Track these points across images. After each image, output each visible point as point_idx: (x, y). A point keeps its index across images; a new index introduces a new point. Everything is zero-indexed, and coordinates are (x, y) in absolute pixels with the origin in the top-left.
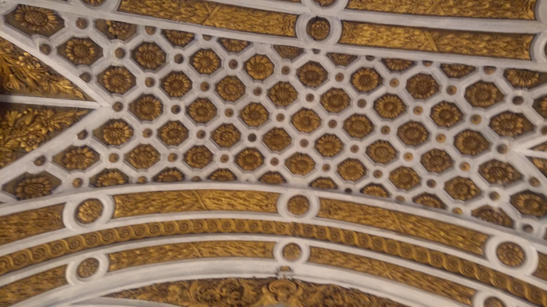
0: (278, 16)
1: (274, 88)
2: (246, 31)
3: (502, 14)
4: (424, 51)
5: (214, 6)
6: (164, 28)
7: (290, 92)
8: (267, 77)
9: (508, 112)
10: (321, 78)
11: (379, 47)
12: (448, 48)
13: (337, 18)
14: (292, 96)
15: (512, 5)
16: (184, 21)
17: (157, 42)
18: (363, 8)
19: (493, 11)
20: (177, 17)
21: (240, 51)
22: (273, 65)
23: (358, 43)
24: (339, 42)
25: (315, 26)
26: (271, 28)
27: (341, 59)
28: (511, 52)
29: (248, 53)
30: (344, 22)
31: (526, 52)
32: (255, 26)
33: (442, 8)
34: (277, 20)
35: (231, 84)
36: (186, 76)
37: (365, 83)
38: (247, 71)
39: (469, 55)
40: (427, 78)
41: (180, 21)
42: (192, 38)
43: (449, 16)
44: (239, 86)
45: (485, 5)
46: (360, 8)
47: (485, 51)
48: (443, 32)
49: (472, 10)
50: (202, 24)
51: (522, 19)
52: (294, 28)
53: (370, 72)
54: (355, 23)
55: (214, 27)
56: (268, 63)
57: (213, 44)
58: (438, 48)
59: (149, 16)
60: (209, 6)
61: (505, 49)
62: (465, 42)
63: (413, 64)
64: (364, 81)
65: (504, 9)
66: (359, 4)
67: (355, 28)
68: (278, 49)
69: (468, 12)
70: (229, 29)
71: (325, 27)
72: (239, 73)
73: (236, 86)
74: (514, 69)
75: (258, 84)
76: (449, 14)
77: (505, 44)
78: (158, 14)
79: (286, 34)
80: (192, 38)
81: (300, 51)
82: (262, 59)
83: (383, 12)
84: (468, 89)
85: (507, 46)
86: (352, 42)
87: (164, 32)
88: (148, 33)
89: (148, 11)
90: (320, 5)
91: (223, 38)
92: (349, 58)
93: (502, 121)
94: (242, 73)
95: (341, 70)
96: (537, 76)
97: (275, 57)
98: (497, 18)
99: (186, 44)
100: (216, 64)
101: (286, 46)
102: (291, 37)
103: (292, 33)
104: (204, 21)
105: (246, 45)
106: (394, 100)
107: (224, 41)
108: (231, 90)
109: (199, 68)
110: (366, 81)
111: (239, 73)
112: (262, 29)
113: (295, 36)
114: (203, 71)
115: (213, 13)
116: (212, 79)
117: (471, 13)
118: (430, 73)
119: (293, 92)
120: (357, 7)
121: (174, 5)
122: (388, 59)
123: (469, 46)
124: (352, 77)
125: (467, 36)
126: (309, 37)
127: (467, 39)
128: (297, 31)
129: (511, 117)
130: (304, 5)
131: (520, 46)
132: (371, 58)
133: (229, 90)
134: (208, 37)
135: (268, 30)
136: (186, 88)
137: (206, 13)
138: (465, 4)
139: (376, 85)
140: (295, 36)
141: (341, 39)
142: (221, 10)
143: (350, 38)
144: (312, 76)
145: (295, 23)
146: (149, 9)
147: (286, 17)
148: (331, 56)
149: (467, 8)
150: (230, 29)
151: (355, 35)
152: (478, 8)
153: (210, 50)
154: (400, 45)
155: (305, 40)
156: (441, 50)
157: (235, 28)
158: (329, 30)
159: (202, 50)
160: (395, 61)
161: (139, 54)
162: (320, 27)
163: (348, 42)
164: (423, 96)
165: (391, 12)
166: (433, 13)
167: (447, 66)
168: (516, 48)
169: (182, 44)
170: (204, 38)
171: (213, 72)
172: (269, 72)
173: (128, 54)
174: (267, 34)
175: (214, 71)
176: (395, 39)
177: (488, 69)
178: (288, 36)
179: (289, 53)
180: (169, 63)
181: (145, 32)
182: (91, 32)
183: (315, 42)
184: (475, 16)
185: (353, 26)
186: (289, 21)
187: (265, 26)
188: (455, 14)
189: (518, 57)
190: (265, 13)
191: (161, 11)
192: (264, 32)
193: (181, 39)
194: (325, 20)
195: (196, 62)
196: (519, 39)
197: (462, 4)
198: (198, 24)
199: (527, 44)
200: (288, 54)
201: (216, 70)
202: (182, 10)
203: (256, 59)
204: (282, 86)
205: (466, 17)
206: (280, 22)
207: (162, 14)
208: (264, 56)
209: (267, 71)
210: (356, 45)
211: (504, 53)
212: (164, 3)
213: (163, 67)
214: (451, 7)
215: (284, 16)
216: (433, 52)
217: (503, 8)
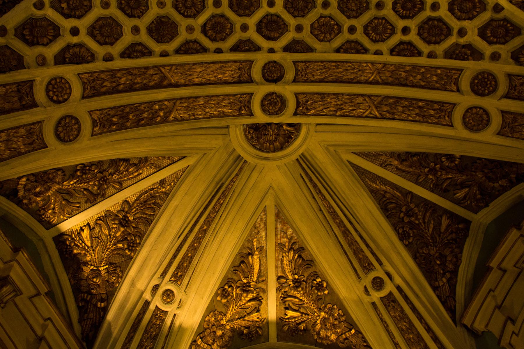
0: (312, 79)
1: (309, 10)
2: (343, 62)
3: (117, 112)
4: (171, 66)
5: (374, 81)
6: (419, 58)
7: (292, 7)
8: (317, 20)
9: (79, 17)
10: (264, 25)
11: (213, 63)
12: (151, 72)
13: (257, 84)
14: (289, 3)
15: (112, 121)
16: (402, 65)
17: (426, 45)
18: (237, 96)
19: (125, 112)
20: (408, 68)
21: (346, 42)
22: (311, 32)
23: (235, 64)
24: (251, 62)
25: (277, 74)
26: (319, 68)
27: (247, 46)
28: (98, 78)
29: (337, 42)
30: (250, 81)
31: (85, 81)
32: (335, 67)
33: (167, 107)
34: (313, 76)
35: (354, 10)
36: (399, 15)
37: (219, 26)
38: (337, 24)
39: (131, 68)
40: (161, 39)
41: (405, 65)
42: (392, 52)
43: (160, 101)
44: (346, 9)
45: (133, 117)
46: (239, 96)
47: (118, 75)
48: (159, 86)
49: (142, 110)
50: (385, 65)
51: (100, 110)
52: (297, 70)
53: (216, 36)
54: (239, 82)
55: (373, 63)
56: (317, 35)
57: (372, 47)
58: (160, 70)
59: (434, 68)
60: (378, 81)
61: (104, 80)
62: (139, 80)
63: (178, 51)
64: (220, 28)
65: (117, 116)
66: (241, 99)
67: (239, 77)
68: (310, 50)
69: (145, 108)
70: (360, 62)
71: (268, 75)
72: (346, 22)
73: (349, 9)
74: (88, 63)
75: (327, 12)
76: (161, 103)
77: (104, 85)
78: (426, 69)
79: (304, 64)
80: (392, 52)
81: (287, 49)
82: (324, 37)
83: (218, 96)
84: (121, 35)
85: (103, 83)
86: (238, 64)
87: (420, 54)
88: (435, 52)
89: (436, 71)
90: (276, 93)
91: (363, 53)
92: (239, 48)
93: (81, 8)
94: (343, 23)
95: (245, 36)
96: (67, 60)
97: (311, 41)
98: (120, 107)
99: (398, 45)
100: (369, 28)
101: (301, 52)
102: (298, 62)
103: (298, 65)
104: (383, 67)
105: (341, 49)
106: (187, 12)
107: (363, 51)
108: (353, 4)
109: (386, 23)
110: (218, 28)
111: (346, 22)
112: (327, 65)
113: (295, 62)
114: (382, 22)
115: (375, 75)
116: (373, 14)
117: (142, 107)
118: (159, 44)
119: (289, 8)
120: (242, 96)
121: (411, 78)
122: (201, 53)
123: (134, 77)
124: (232, 31)
125: (137, 86)
126: (281, 63)
127: (137, 83)
128: (294, 67)
129: (75, 13)
130: (291, 92)
131: (92, 85)
132: (217, 51)
133: (356, 4)
134: (378, 53)
135: (322, 66)
136: (399, 3)
137: (381, 75)
138: (150, 114)
139: (207, 25)
140: (295, 62)
141: (251, 66)
142: (367, 78)
143: (242, 68)
144: (273, 26)
145: (296, 74)
146: (434, 73)
147: (305, 78)
148: (258, 49)
149: (147, 111)
150: (358, 62)
151: (237, 71)
152: (137, 113)
153: (375, 41)
154: (194, 67)
155: (285, 60)
156: (156, 69)
157: (353, 64)
158: (263, 72)
159: (383, 41)
160: (194, 52)
161: (444, 33)
162: (273, 74)
163: (243, 64)
164: (161, 20)
165: (210, 97)
166: (174, 101)
167: (147, 54)
168: (95, 83)
169: (403, 45)
170: (382, 52)
171: (372, 21)
172: (316, 25)
173: (455, 32)
174: (322, 62)
175: (371, 22)
176: (201, 72)
177: (108, 58)
178: (302, 62)
179: (298, 47)
180: (416, 26)
181: (438, 53)
182: (488, 50)
183: (275, 59)
184: (139, 105)
185: (241, 79)
186: (302, 76)
187: (324, 68)
188: (156, 104)
189: (90, 75)
190: (326, 80)
191: (423, 73)
192: (325, 63)
193: (403, 50)
194: (268, 81)
195: (389, 29)
196: (95, 91)
197: (152, 113)
198: (388, 64)
199: (88, 89)
200: (299, 45)
201: (369, 23)
202: (403, 74)
203: (330, 36)
204: (302, 13)
205: (145, 103)
206: (311, 73)
207: (423, 70)
208: (321, 41)
209: (318, 27)
210: (235, 62)
211: (103, 76)
212: (420, 79)
213: (422, 22)
214: (160, 109)
215: (307, 80)
216: (164, 66)
217: (118, 117)
